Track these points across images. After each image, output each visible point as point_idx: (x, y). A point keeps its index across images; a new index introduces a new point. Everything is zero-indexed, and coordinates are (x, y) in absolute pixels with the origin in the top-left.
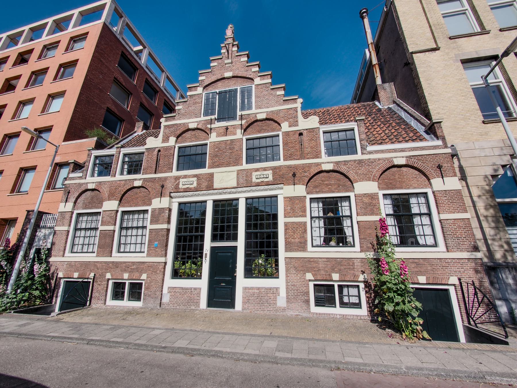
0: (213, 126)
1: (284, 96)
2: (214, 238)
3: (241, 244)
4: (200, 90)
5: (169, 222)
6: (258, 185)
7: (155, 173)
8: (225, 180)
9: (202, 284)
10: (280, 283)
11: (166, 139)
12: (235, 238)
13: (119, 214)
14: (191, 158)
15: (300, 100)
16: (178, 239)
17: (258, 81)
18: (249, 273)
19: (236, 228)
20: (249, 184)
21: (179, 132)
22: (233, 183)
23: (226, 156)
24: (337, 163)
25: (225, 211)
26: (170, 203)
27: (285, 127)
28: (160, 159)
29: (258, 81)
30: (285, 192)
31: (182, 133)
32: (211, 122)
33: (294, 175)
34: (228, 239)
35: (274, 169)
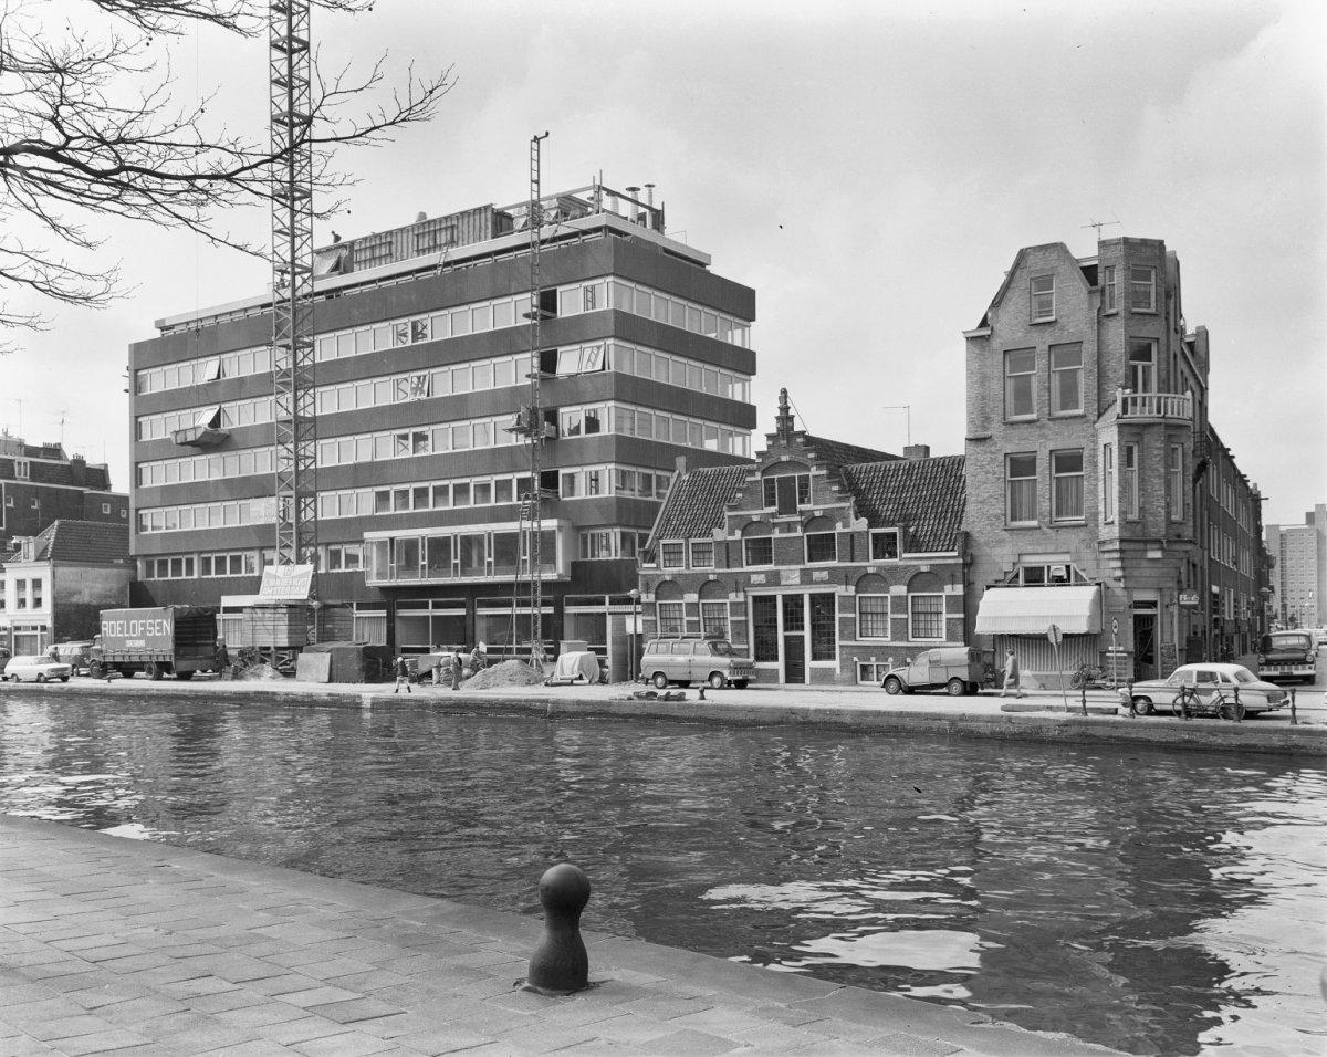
0: (776, 520)
1: (840, 492)
2: (786, 629)
3: (807, 633)
4: (758, 476)
5: (746, 615)
6: (816, 583)
7: (728, 567)
8: (791, 579)
9: (779, 665)
10: (835, 664)
11: (731, 533)
12: (802, 628)
13: (701, 606)
14: (761, 552)
15: (853, 499)
16: (756, 627)
17: (814, 471)
18: (815, 657)
19: (802, 620)
20: (811, 582)
21: (743, 525)
22: (798, 581)
23: (789, 555)
24: (879, 567)
25: (793, 603)
26: (746, 597)
27: (839, 528)
28: (728, 553)
29: (814, 471)
30: (840, 591)
31: (747, 526)
32: (773, 515)
33: (847, 577)
34: (797, 629)
35: (831, 570)
